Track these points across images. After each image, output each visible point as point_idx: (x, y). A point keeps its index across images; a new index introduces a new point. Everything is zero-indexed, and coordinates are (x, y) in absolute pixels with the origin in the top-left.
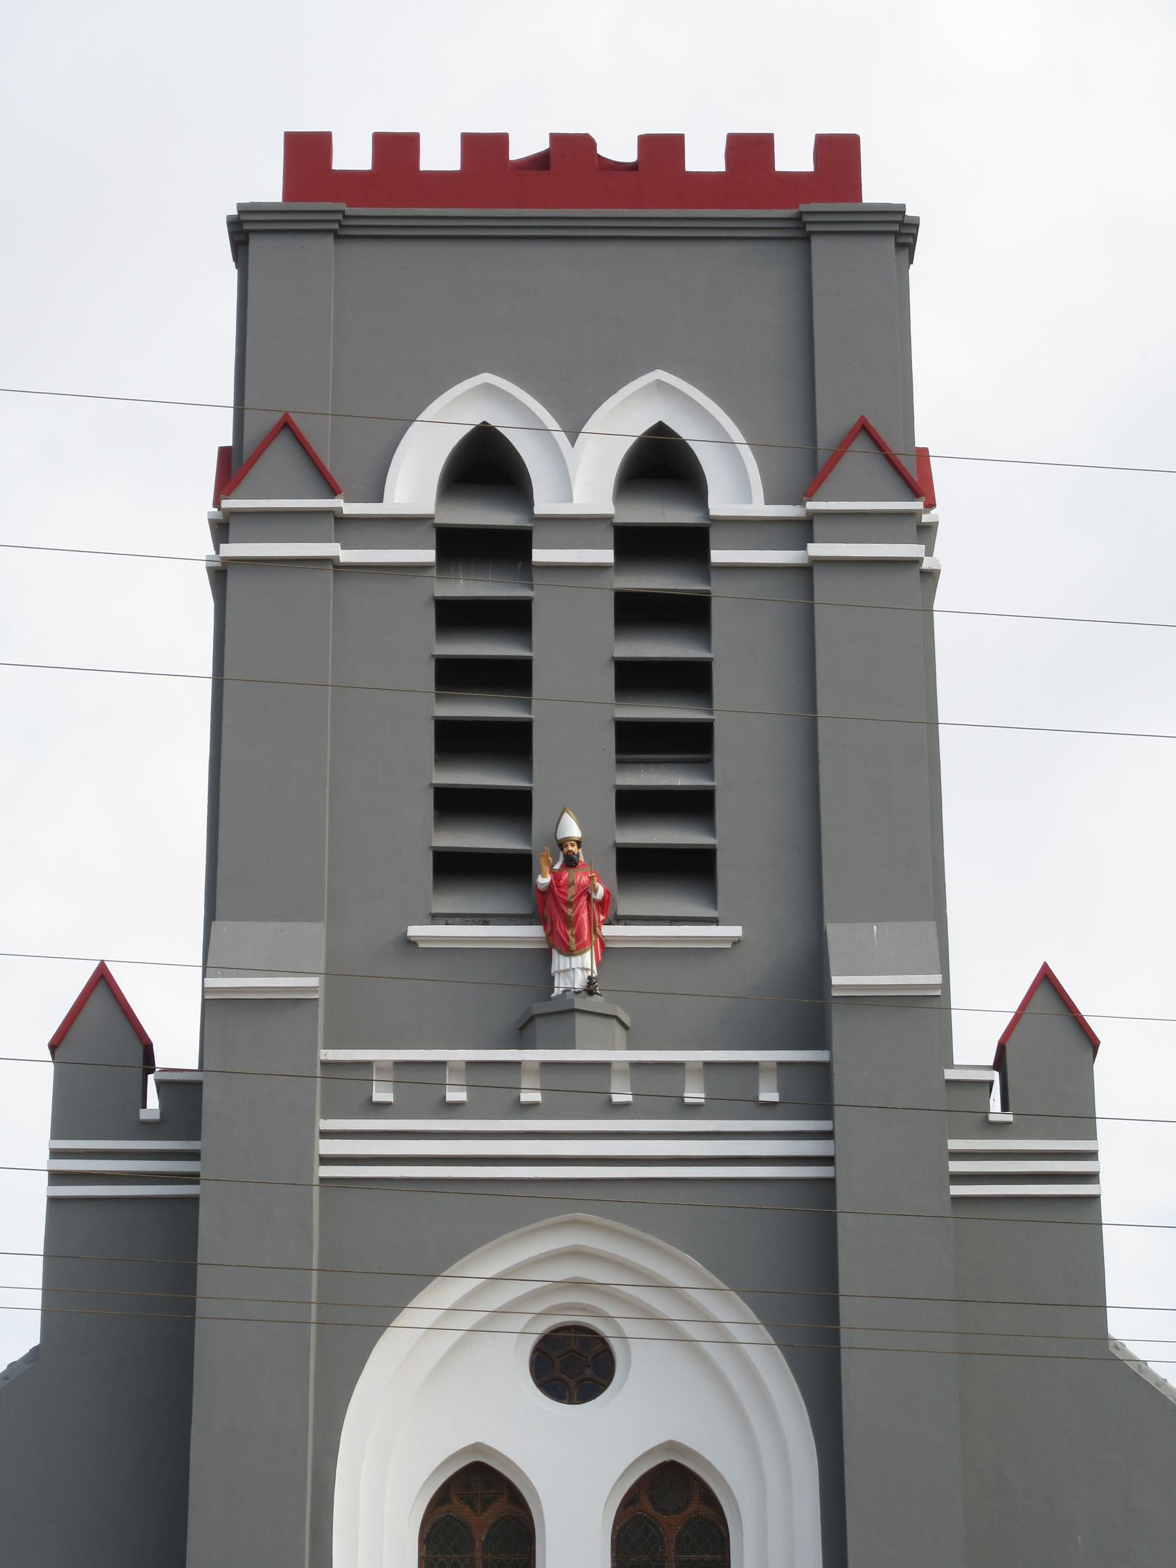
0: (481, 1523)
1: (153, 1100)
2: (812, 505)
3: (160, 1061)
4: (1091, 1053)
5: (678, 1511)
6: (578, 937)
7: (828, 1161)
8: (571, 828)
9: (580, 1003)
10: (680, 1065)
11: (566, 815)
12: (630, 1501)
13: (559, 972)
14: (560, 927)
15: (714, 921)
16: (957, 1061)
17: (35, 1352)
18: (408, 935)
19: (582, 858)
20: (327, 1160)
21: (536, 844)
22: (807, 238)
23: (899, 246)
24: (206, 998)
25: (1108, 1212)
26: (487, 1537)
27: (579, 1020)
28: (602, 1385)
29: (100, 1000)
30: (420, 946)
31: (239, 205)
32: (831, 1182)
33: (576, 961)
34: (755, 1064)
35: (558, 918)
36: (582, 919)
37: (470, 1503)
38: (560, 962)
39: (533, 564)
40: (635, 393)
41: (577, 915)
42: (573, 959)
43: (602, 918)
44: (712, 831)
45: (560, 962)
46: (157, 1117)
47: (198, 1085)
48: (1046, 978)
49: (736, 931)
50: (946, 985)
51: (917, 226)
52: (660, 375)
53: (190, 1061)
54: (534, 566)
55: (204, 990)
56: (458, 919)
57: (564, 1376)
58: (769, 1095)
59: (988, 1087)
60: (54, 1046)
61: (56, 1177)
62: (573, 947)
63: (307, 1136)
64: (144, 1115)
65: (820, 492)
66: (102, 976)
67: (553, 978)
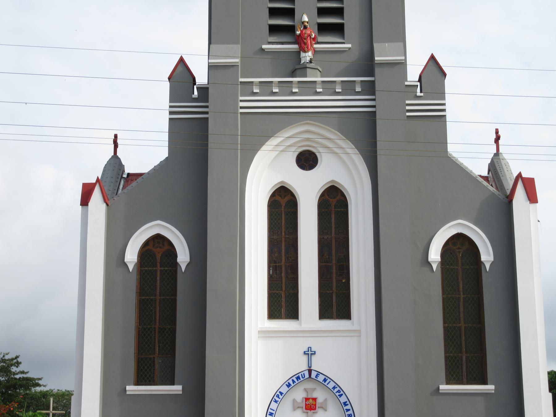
0: (283, 201)
1: (196, 93)
4: (444, 77)
5: (335, 198)
6: (307, 48)
7: (374, 106)
8: (305, 18)
9: (308, 65)
10: (335, 82)
11: (304, 15)
12: (322, 195)
13: (302, 57)
14: (303, 45)
16: (408, 80)
17: (167, 158)
18: (262, 47)
19: (308, 27)
20: (241, 108)
21: (296, 23)
25: (448, 119)
26: (285, 205)
27: (308, 69)
30: (266, 51)
32: (374, 113)
33: (307, 54)
34: (355, 81)
36: (309, 43)
37: (280, 196)
38: (303, 54)
41: (307, 42)
42: (306, 53)
43: (314, 42)
44: (343, 19)
45: (303, 54)
46: (197, 97)
47: (207, 88)
48: (432, 58)
50: (406, 59)
53: (206, 82)
56: (275, 43)
57: (305, 164)
58: (358, 89)
59: (417, 87)
60: (169, 78)
61: (171, 113)
62: (306, 50)
63: (236, 101)
64: (193, 96)
66: (182, 59)
67: (301, 59)
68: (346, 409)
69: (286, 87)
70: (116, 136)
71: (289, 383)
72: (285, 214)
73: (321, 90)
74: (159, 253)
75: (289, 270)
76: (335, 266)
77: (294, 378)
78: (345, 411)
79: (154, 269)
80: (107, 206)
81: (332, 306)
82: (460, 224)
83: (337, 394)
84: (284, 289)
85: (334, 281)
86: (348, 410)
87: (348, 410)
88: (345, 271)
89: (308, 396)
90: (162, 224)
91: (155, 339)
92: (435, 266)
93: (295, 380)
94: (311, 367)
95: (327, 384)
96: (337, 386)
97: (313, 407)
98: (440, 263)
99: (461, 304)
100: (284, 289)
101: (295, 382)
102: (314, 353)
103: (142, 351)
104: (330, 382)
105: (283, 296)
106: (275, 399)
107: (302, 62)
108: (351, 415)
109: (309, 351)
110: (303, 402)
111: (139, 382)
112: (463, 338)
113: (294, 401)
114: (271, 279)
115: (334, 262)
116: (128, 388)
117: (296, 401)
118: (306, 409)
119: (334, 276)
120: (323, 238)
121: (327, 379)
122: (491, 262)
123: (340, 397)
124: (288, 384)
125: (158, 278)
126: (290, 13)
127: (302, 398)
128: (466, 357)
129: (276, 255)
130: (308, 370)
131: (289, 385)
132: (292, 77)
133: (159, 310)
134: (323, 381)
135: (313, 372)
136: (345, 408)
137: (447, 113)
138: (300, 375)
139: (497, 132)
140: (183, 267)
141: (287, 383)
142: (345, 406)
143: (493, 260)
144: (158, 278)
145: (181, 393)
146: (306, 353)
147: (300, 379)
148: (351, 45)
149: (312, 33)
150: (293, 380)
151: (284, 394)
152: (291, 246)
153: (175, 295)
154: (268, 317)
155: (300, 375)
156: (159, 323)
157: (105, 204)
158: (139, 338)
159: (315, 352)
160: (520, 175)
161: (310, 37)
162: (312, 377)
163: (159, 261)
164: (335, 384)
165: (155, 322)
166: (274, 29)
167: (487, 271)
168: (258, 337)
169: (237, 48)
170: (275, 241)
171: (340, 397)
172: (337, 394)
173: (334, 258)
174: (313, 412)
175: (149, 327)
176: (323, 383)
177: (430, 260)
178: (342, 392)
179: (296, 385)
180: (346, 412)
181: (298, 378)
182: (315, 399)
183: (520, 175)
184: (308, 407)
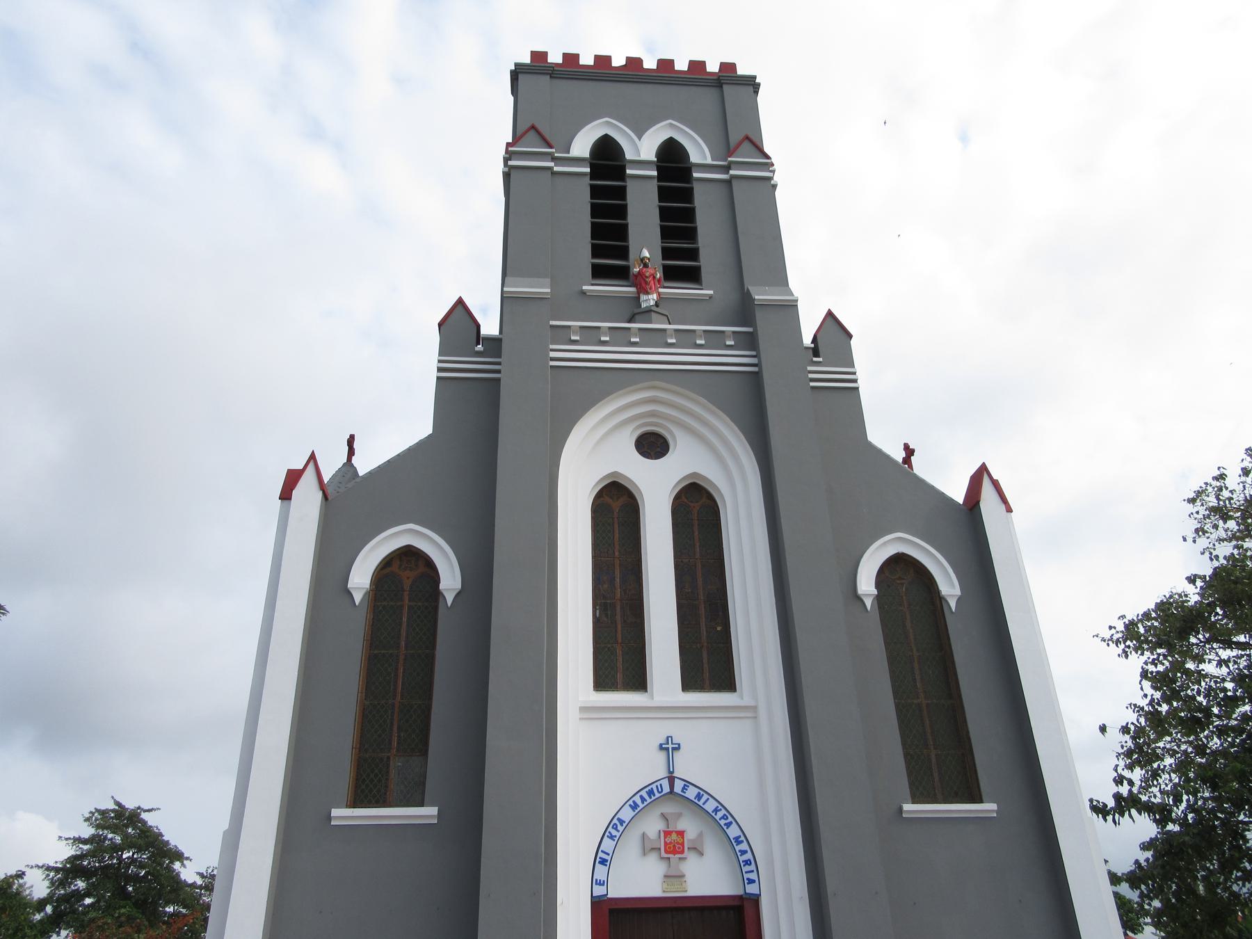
0: (616, 505)
2: (729, 159)
3: (485, 331)
5: (697, 502)
6: (650, 289)
8: (646, 253)
9: (655, 309)
14: (644, 285)
15: (702, 289)
20: (553, 359)
22: (722, 87)
23: (754, 92)
24: (505, 296)
26: (619, 510)
27: (653, 313)
29: (460, 308)
31: (515, 63)
33: (650, 297)
34: (723, 332)
35: (643, 282)
37: (611, 498)
38: (643, 297)
45: (643, 297)
51: (759, 85)
52: (670, 121)
55: (502, 292)
60: (440, 325)
61: (440, 370)
65: (734, 154)
68: (740, 851)
69: (620, 336)
70: (352, 438)
71: (634, 802)
73: (674, 341)
74: (408, 578)
76: (703, 606)
77: (644, 793)
78: (739, 854)
80: (323, 499)
81: (703, 670)
83: (722, 822)
84: (620, 641)
86: (744, 852)
87: (744, 852)
88: (721, 613)
91: (392, 724)
92: (868, 603)
93: (646, 796)
94: (673, 772)
95: (704, 804)
96: (720, 807)
97: (679, 848)
99: (916, 665)
100: (620, 641)
101: (646, 801)
102: (677, 746)
103: (366, 746)
105: (619, 652)
106: (609, 832)
107: (644, 305)
111: (357, 801)
113: (644, 836)
114: (597, 623)
115: (702, 597)
116: (335, 812)
118: (666, 852)
120: (682, 561)
121: (703, 795)
124: (632, 804)
125: (405, 619)
126: (623, 253)
129: (606, 586)
132: (629, 322)
136: (738, 848)
137: (862, 384)
138: (654, 786)
139: (906, 447)
140: (450, 600)
141: (631, 802)
143: (960, 594)
144: (405, 619)
146: (664, 746)
147: (654, 795)
151: (626, 823)
157: (321, 492)
159: (679, 745)
160: (983, 470)
161: (654, 277)
162: (675, 790)
163: (407, 586)
164: (718, 805)
166: (599, 273)
167: (952, 612)
168: (580, 719)
169: (548, 281)
170: (605, 564)
171: (727, 828)
172: (722, 822)
174: (680, 858)
176: (696, 801)
177: (860, 592)
178: (730, 819)
179: (641, 812)
180: (741, 855)
181: (651, 793)
182: (681, 834)
183: (983, 470)
184: (670, 848)
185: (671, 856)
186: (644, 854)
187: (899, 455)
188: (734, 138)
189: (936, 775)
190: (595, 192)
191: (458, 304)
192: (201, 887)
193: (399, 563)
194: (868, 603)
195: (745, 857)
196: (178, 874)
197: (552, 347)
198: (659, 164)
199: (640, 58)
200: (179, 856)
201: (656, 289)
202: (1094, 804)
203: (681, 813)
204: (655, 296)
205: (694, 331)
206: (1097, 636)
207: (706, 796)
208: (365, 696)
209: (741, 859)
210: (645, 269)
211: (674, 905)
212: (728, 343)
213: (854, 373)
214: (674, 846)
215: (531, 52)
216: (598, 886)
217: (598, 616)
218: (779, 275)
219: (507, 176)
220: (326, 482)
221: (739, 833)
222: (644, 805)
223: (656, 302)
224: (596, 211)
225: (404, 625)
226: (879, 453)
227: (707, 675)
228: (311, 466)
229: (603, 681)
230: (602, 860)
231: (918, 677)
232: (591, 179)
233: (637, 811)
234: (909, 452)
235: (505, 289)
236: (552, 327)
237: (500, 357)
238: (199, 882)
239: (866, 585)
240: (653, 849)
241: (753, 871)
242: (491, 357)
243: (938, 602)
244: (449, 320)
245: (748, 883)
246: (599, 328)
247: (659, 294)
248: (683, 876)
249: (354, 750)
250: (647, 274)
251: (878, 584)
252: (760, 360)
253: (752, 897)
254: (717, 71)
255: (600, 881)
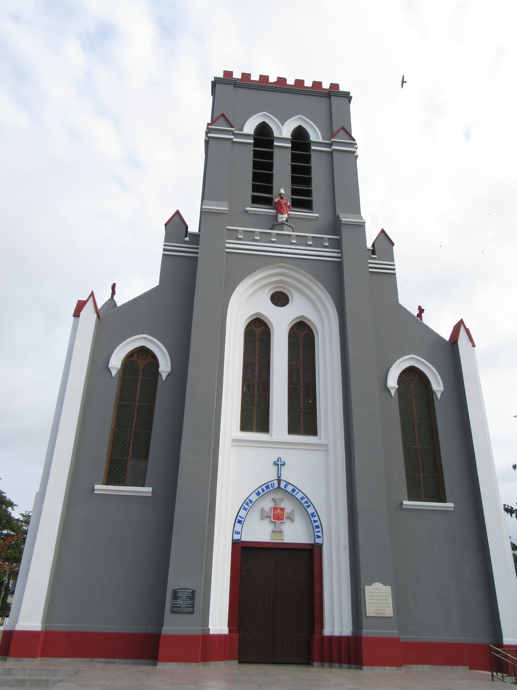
0: (258, 331)
2: (332, 140)
3: (190, 230)
5: (303, 332)
6: (284, 211)
8: (282, 191)
13: (279, 218)
14: (280, 208)
15: (312, 213)
24: (202, 210)
27: (284, 226)
28: (285, 304)
30: (249, 212)
31: (214, 77)
33: (283, 216)
34: (323, 238)
37: (256, 327)
38: (280, 216)
39: (274, 145)
40: (295, 119)
42: (283, 215)
43: (288, 210)
45: (280, 216)
48: (383, 231)
49: (317, 215)
54: (275, 146)
58: (326, 244)
60: (166, 225)
61: (165, 250)
62: (283, 212)
65: (334, 138)
67: (278, 221)
68: (314, 521)
69: (266, 237)
72: (259, 341)
73: (295, 241)
74: (142, 364)
75: (261, 389)
76: (302, 388)
77: (264, 487)
78: (313, 522)
79: (136, 377)
80: (98, 318)
82: (412, 358)
83: (305, 505)
84: (256, 405)
85: (302, 400)
86: (315, 521)
87: (315, 521)
88: (312, 393)
89: (276, 506)
90: (148, 338)
92: (393, 392)
93: (265, 489)
94: (280, 477)
95: (296, 495)
96: (305, 497)
97: (281, 517)
98: (397, 390)
100: (256, 405)
101: (265, 491)
102: (283, 463)
104: (298, 492)
105: (255, 411)
106: (244, 507)
107: (280, 220)
108: (318, 527)
109: (278, 462)
110: (271, 511)
111: (108, 482)
112: (420, 458)
113: (262, 509)
115: (302, 384)
116: (97, 487)
117: (265, 511)
118: (274, 519)
119: (302, 397)
120: (292, 364)
121: (296, 490)
122: (442, 392)
123: (308, 508)
124: (257, 493)
125: (139, 386)
126: (270, 190)
127: (270, 507)
128: (423, 476)
129: (250, 375)
130: (277, 480)
131: (258, 494)
133: (137, 415)
134: (291, 491)
135: (282, 482)
136: (313, 519)
138: (269, 484)
140: (164, 376)
141: (256, 491)
142: (312, 517)
144: (139, 386)
145: (151, 495)
146: (276, 463)
147: (269, 488)
148: (318, 215)
149: (288, 202)
150: (262, 489)
151: (253, 502)
152: (263, 368)
153: (153, 401)
154: (240, 429)
155: (269, 484)
156: (135, 427)
157: (96, 314)
158: (113, 440)
159: (285, 462)
161: (286, 205)
163: (141, 368)
164: (303, 495)
165: (132, 427)
166: (256, 200)
168: (232, 445)
171: (308, 508)
172: (305, 505)
173: (302, 381)
174: (281, 522)
175: (125, 430)
176: (292, 493)
178: (309, 503)
181: (268, 487)
182: (282, 509)
183: (461, 323)
184: (276, 517)
185: (276, 521)
186: (262, 519)
187: (415, 312)
188: (335, 128)
189: (422, 487)
190: (256, 154)
191: (176, 213)
192: (22, 522)
193: (137, 355)
194: (393, 392)
195: (316, 524)
196: (10, 514)
197: (227, 241)
198: (292, 140)
199: (285, 78)
200: (11, 504)
201: (287, 212)
202: (506, 507)
203: (283, 499)
204: (286, 216)
205: (306, 237)
206: (516, 417)
207: (297, 491)
208: (116, 426)
209: (314, 524)
210: (281, 200)
211: (276, 547)
212: (325, 244)
213: (394, 265)
214: (278, 516)
215: (224, 71)
216: (236, 534)
217: (244, 390)
218: (356, 209)
219: (207, 142)
220: (99, 309)
221: (314, 511)
222: (264, 493)
223: (287, 219)
224: (256, 165)
225: (139, 389)
226: (405, 310)
227: (302, 426)
228: (91, 300)
229: (245, 426)
230: (239, 521)
231: (416, 434)
232: (254, 147)
233: (259, 496)
234: (421, 310)
235: (203, 207)
236: (228, 230)
237: (199, 245)
238: (21, 518)
239: (392, 382)
240: (267, 517)
241: (320, 532)
242: (195, 245)
243: (431, 393)
244: (171, 223)
245: (317, 538)
246: (254, 232)
247: (288, 214)
248: (282, 532)
249: (108, 454)
250: (283, 203)
251: (399, 382)
252: (342, 255)
253: (319, 545)
254: (328, 88)
255: (237, 531)
